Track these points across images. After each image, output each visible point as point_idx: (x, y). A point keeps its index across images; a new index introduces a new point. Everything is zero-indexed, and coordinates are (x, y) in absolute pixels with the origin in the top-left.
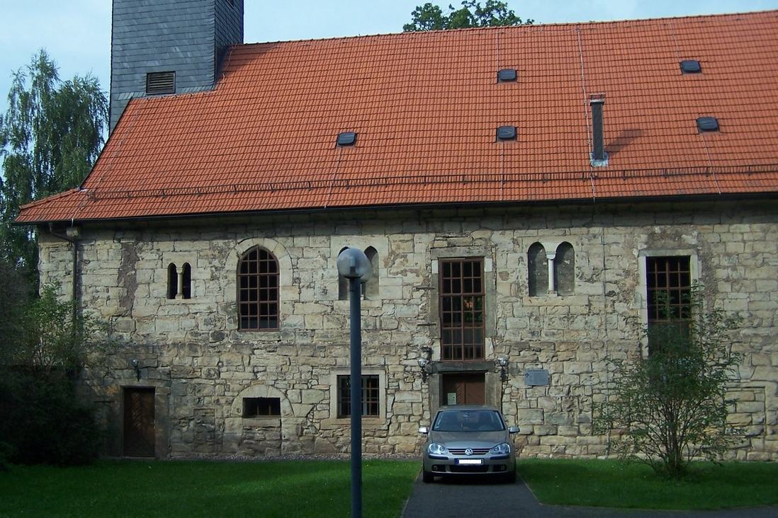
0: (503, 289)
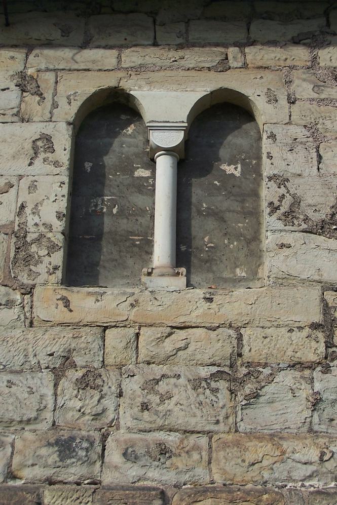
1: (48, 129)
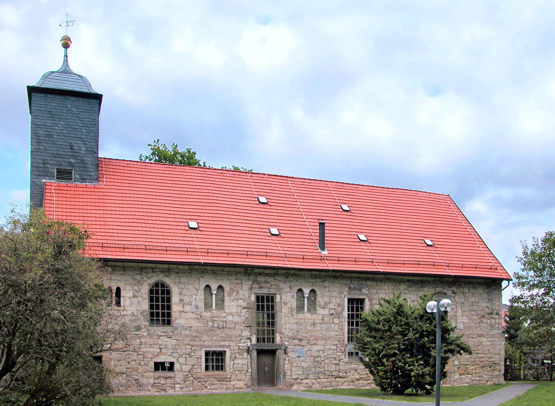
0: (285, 310)
1: (293, 294)
